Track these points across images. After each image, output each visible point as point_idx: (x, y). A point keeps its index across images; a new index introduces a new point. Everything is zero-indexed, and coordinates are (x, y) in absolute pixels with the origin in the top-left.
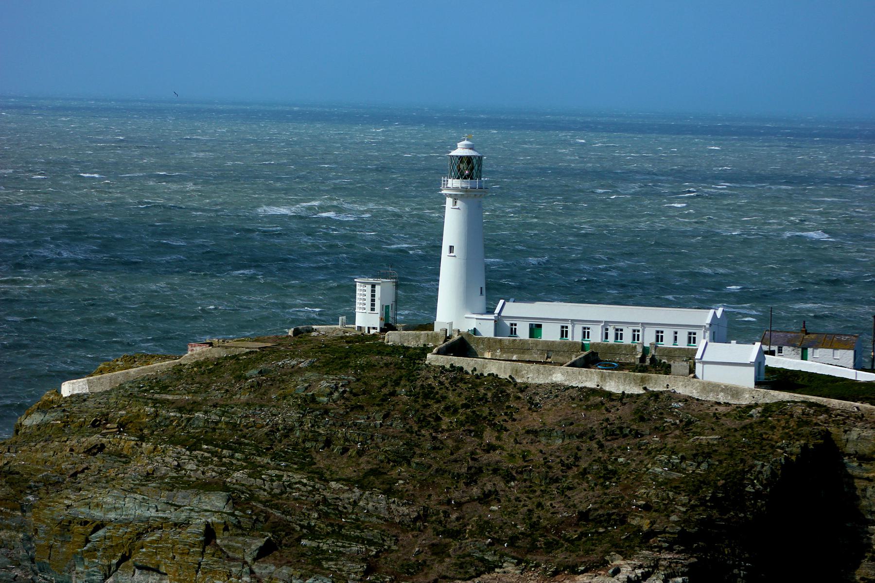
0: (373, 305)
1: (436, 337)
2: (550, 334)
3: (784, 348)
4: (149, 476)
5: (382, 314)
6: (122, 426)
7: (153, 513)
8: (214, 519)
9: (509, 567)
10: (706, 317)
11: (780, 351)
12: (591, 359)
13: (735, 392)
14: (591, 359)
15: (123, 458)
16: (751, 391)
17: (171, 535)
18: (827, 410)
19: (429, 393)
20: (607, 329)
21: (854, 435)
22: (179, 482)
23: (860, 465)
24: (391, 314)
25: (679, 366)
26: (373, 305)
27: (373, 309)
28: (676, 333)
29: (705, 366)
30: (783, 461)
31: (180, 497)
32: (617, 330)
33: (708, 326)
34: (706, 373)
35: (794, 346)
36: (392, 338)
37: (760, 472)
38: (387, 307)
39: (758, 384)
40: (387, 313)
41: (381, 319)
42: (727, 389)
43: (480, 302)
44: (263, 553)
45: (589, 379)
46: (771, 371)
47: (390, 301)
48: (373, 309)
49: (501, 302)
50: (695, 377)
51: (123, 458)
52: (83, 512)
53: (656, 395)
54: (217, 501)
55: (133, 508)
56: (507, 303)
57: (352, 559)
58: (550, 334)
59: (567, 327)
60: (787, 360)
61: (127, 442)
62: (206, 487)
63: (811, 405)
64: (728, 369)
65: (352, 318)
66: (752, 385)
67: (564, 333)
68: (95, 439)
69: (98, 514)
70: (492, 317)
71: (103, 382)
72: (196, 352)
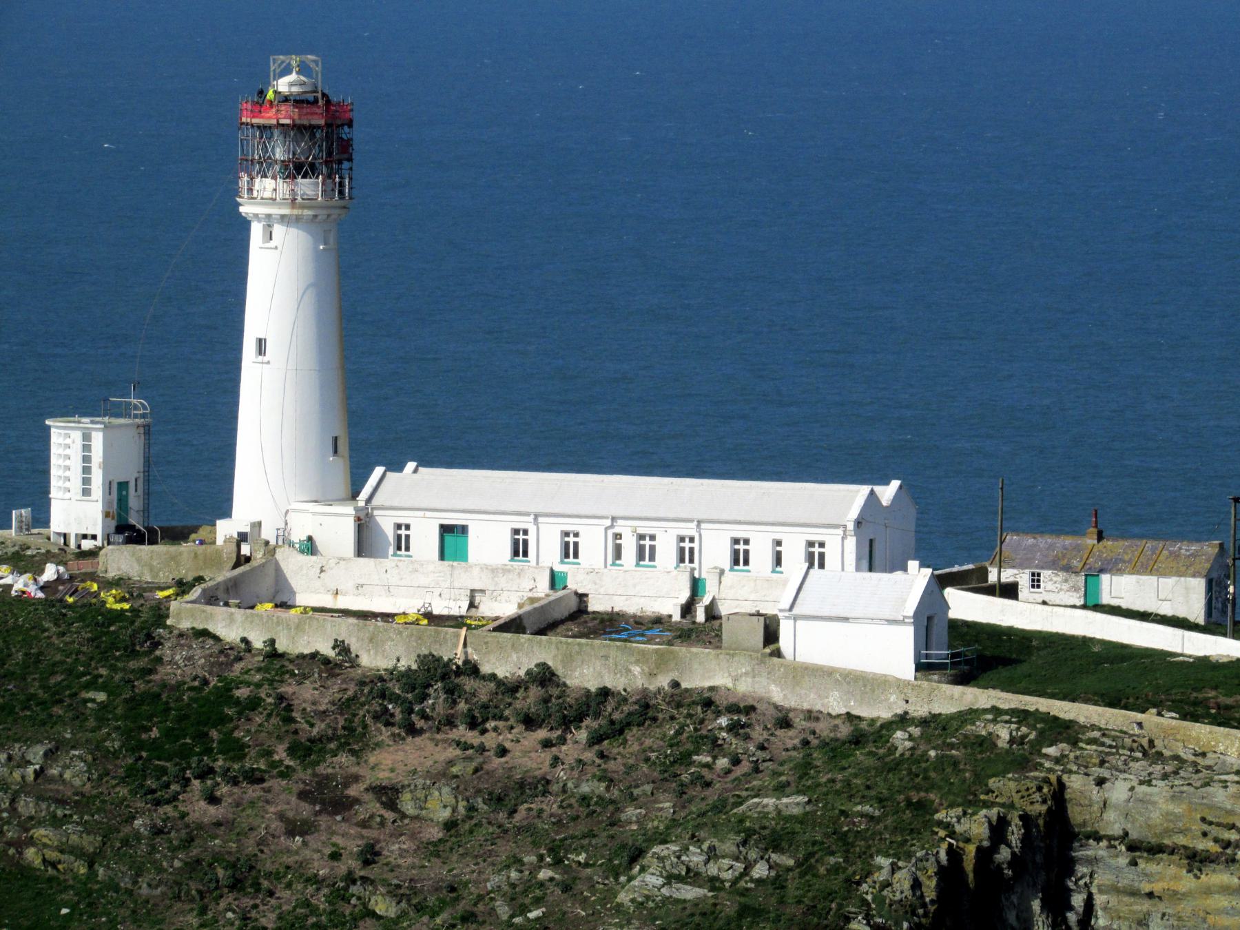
0: (86, 481)
1: (215, 561)
3: (1045, 574)
5: (107, 503)
11: (1036, 582)
16: (900, 684)
20: (618, 536)
21: (1118, 791)
23: (1134, 863)
24: (135, 501)
26: (86, 481)
27: (86, 492)
28: (779, 543)
29: (799, 623)
30: (943, 856)
32: (642, 537)
33: (851, 526)
34: (803, 643)
35: (1068, 569)
37: (887, 884)
38: (123, 486)
39: (923, 667)
40: (122, 502)
41: (107, 515)
43: (339, 469)
46: (963, 631)
47: (131, 471)
48: (86, 492)
49: (379, 471)
50: (778, 654)
56: (389, 474)
59: (526, 532)
60: (1044, 607)
63: (1022, 716)
65: (41, 517)
66: (906, 669)
67: (519, 549)
70: (350, 510)
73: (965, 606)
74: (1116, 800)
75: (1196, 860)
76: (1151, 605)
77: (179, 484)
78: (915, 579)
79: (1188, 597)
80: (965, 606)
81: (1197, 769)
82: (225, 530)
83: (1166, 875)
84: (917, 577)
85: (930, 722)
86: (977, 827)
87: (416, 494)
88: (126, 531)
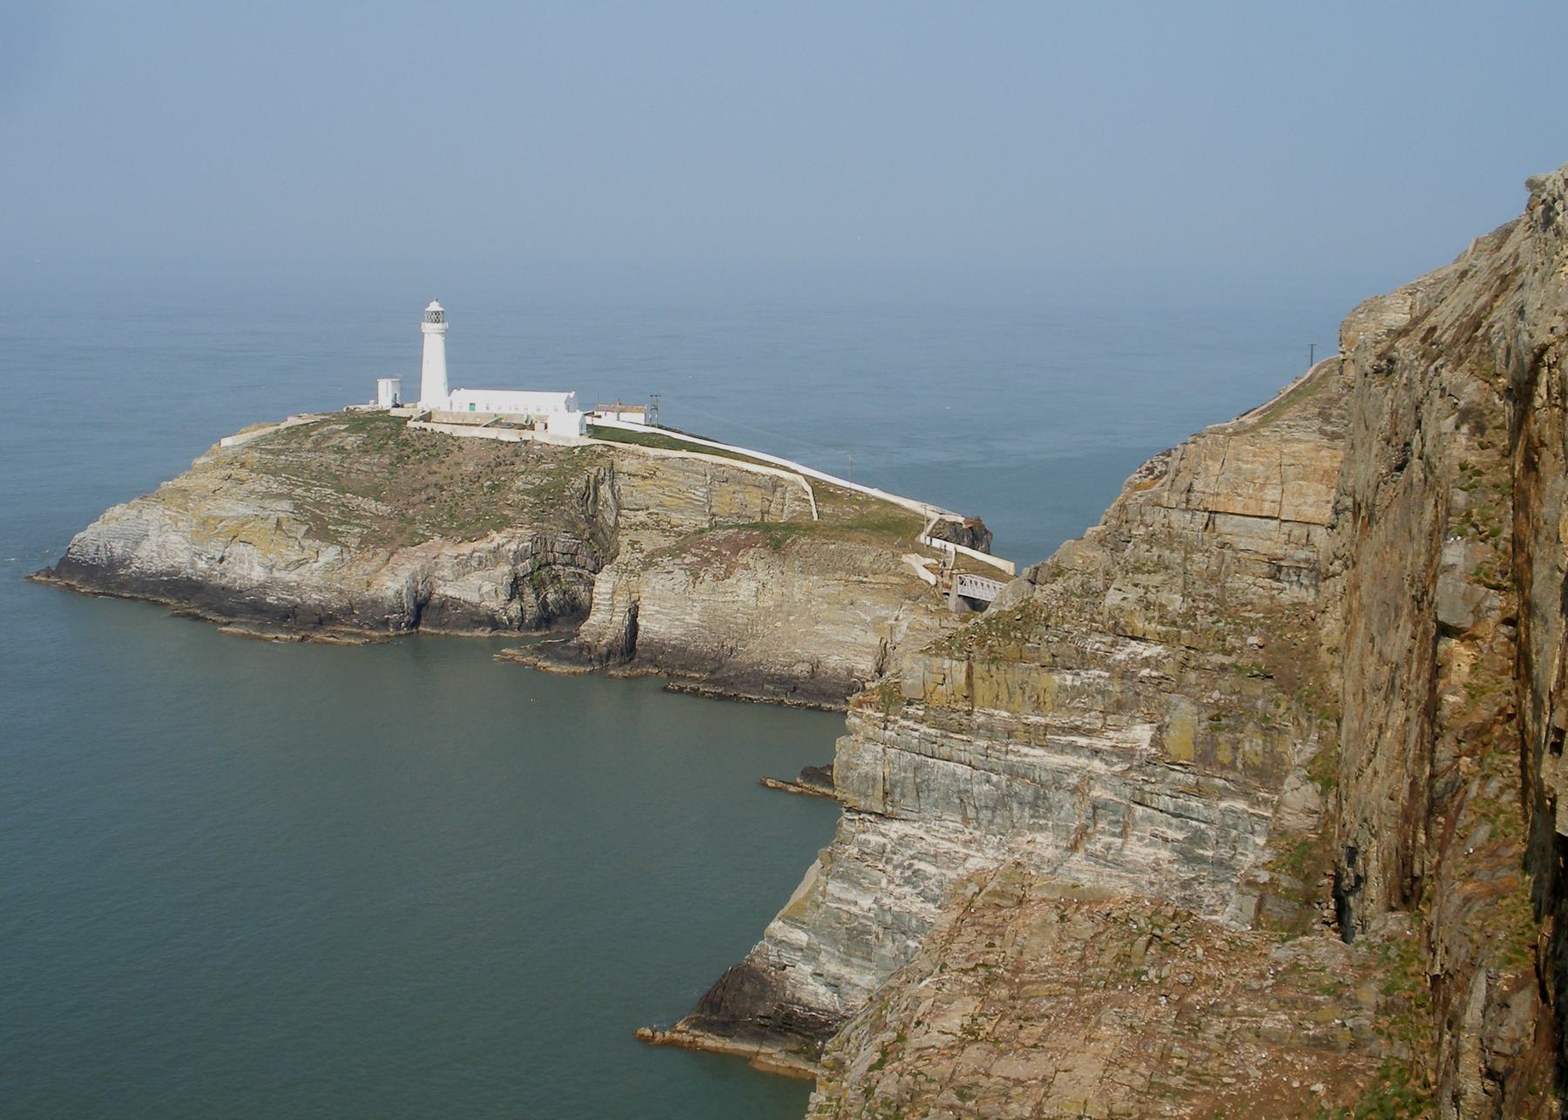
2: (480, 409)
4: (252, 492)
6: (243, 465)
7: (250, 512)
8: (282, 515)
9: (437, 538)
10: (559, 398)
12: (497, 423)
13: (569, 440)
14: (497, 423)
15: (242, 482)
17: (260, 524)
18: (614, 448)
19: (406, 443)
22: (268, 495)
25: (539, 426)
31: (266, 503)
36: (395, 412)
42: (563, 438)
44: (307, 534)
45: (492, 433)
51: (242, 482)
52: (217, 513)
53: (526, 442)
54: (286, 505)
55: (241, 510)
57: (354, 536)
58: (480, 409)
60: (608, 420)
61: (243, 473)
62: (280, 496)
68: (229, 472)
69: (224, 514)
72: (293, 421)
73: (589, 420)
74: (628, 464)
75: (644, 478)
76: (633, 421)
78: (579, 414)
79: (640, 418)
80: (589, 420)
81: (645, 456)
82: (420, 405)
83: (637, 481)
84: (579, 414)
85: (583, 449)
86: (594, 471)
87: (464, 397)
88: (397, 406)
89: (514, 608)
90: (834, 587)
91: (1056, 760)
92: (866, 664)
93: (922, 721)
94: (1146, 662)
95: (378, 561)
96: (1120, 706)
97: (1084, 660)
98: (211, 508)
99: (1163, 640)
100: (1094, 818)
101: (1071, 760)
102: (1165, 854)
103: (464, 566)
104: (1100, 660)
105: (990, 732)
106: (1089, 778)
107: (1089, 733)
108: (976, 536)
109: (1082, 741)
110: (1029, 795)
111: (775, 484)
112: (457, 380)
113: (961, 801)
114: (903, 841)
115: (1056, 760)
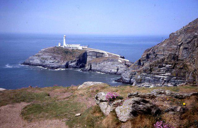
60: (84, 47)
64: (80, 48)
71: (44, 50)
74: (88, 52)
77: (62, 44)
89: (77, 66)
90: (112, 63)
91: (160, 76)
92: (116, 70)
93: (145, 73)
94: (170, 66)
95: (62, 62)
96: (167, 71)
97: (163, 66)
98: (42, 57)
99: (172, 64)
100: (165, 82)
101: (162, 76)
102: (172, 85)
103: (72, 62)
104: (164, 67)
105: (153, 74)
106: (164, 78)
107: (164, 74)
108: (123, 58)
109: (163, 74)
110: (157, 80)
111: (103, 53)
112: (67, 43)
113: (149, 81)
114: (143, 85)
115: (160, 76)
